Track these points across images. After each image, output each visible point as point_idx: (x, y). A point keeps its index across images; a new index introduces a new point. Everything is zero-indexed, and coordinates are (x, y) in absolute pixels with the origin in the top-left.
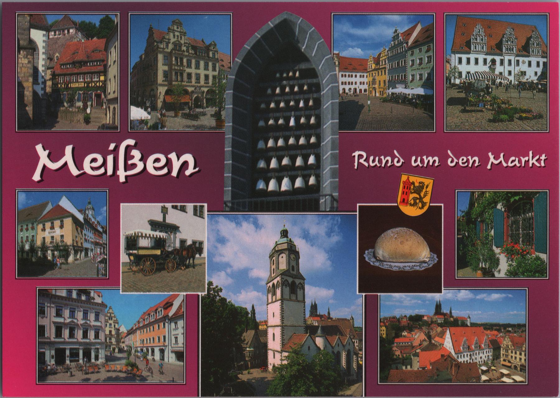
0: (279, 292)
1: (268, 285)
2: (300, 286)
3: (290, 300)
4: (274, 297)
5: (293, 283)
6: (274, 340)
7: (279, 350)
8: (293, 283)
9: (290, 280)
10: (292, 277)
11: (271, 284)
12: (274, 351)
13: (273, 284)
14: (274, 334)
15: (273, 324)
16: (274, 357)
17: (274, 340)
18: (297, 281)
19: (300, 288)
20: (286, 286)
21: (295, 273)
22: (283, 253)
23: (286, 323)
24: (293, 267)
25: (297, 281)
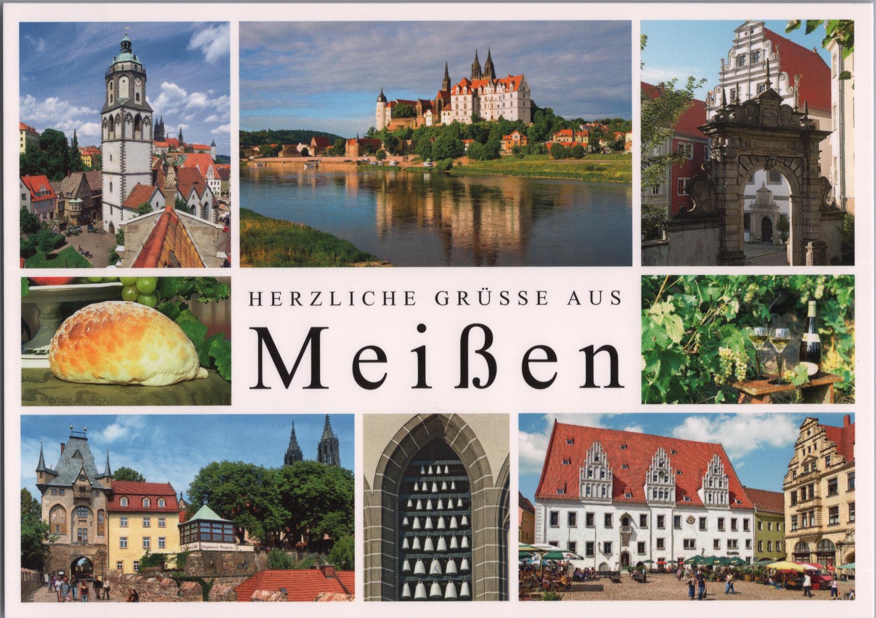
0: (118, 129)
1: (104, 116)
2: (147, 120)
3: (134, 140)
4: (112, 133)
5: (138, 117)
6: (111, 190)
7: (119, 205)
8: (138, 117)
9: (134, 113)
10: (138, 110)
11: (107, 116)
12: (111, 206)
13: (111, 117)
14: (111, 183)
15: (110, 170)
16: (111, 213)
17: (111, 190)
18: (143, 115)
19: (147, 124)
20: (129, 121)
21: (140, 103)
22: (124, 75)
23: (128, 170)
24: (138, 94)
25: (143, 115)
